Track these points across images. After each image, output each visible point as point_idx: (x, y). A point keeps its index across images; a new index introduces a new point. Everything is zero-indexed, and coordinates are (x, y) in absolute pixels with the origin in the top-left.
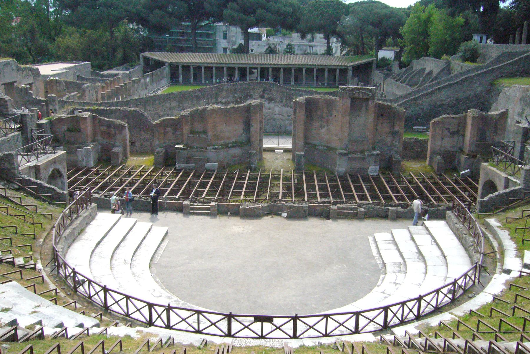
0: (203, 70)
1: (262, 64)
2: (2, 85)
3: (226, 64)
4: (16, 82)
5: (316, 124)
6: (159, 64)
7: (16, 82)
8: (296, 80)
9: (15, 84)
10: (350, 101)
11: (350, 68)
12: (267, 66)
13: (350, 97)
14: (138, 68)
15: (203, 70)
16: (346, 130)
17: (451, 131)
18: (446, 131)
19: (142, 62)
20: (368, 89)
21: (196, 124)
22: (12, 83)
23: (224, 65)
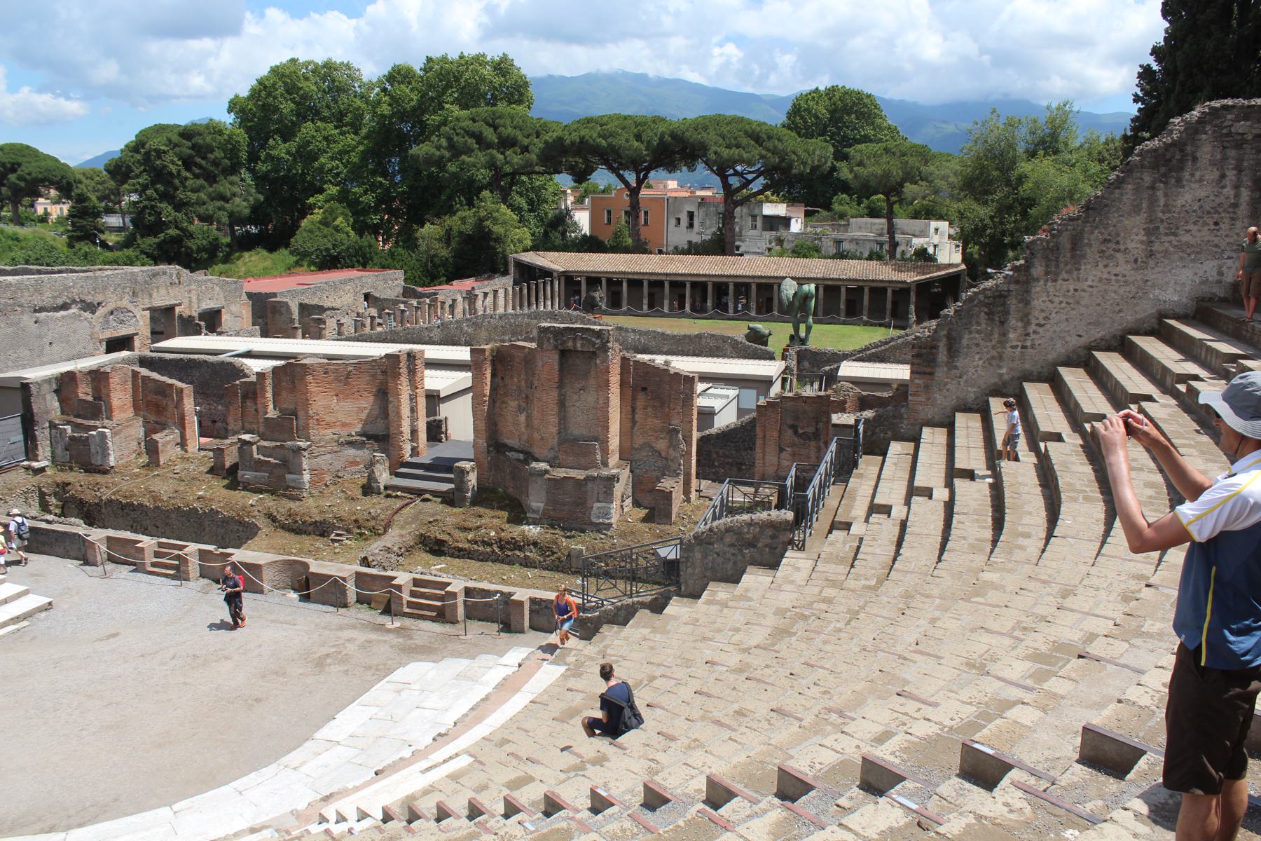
0: (625, 285)
1: (737, 276)
2: (144, 310)
3: (667, 275)
4: (180, 305)
5: (513, 404)
6: (546, 273)
7: (180, 305)
8: (651, 306)
9: (178, 310)
10: (557, 357)
11: (913, 288)
12: (724, 280)
13: (556, 347)
14: (508, 281)
15: (625, 285)
16: (553, 419)
17: (800, 431)
18: (790, 432)
19: (512, 270)
20: (593, 330)
21: (284, 394)
22: (170, 310)
23: (663, 278)
